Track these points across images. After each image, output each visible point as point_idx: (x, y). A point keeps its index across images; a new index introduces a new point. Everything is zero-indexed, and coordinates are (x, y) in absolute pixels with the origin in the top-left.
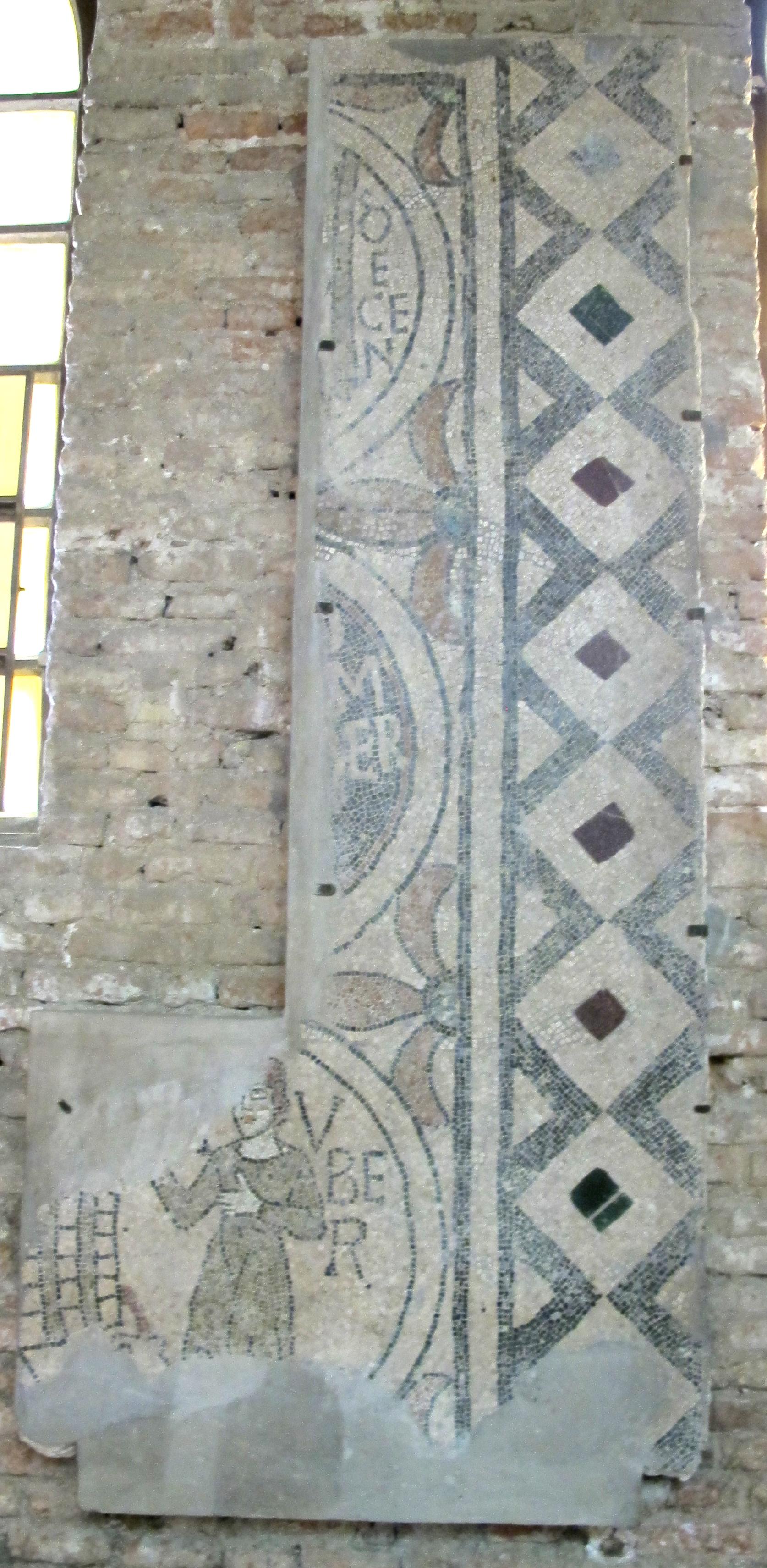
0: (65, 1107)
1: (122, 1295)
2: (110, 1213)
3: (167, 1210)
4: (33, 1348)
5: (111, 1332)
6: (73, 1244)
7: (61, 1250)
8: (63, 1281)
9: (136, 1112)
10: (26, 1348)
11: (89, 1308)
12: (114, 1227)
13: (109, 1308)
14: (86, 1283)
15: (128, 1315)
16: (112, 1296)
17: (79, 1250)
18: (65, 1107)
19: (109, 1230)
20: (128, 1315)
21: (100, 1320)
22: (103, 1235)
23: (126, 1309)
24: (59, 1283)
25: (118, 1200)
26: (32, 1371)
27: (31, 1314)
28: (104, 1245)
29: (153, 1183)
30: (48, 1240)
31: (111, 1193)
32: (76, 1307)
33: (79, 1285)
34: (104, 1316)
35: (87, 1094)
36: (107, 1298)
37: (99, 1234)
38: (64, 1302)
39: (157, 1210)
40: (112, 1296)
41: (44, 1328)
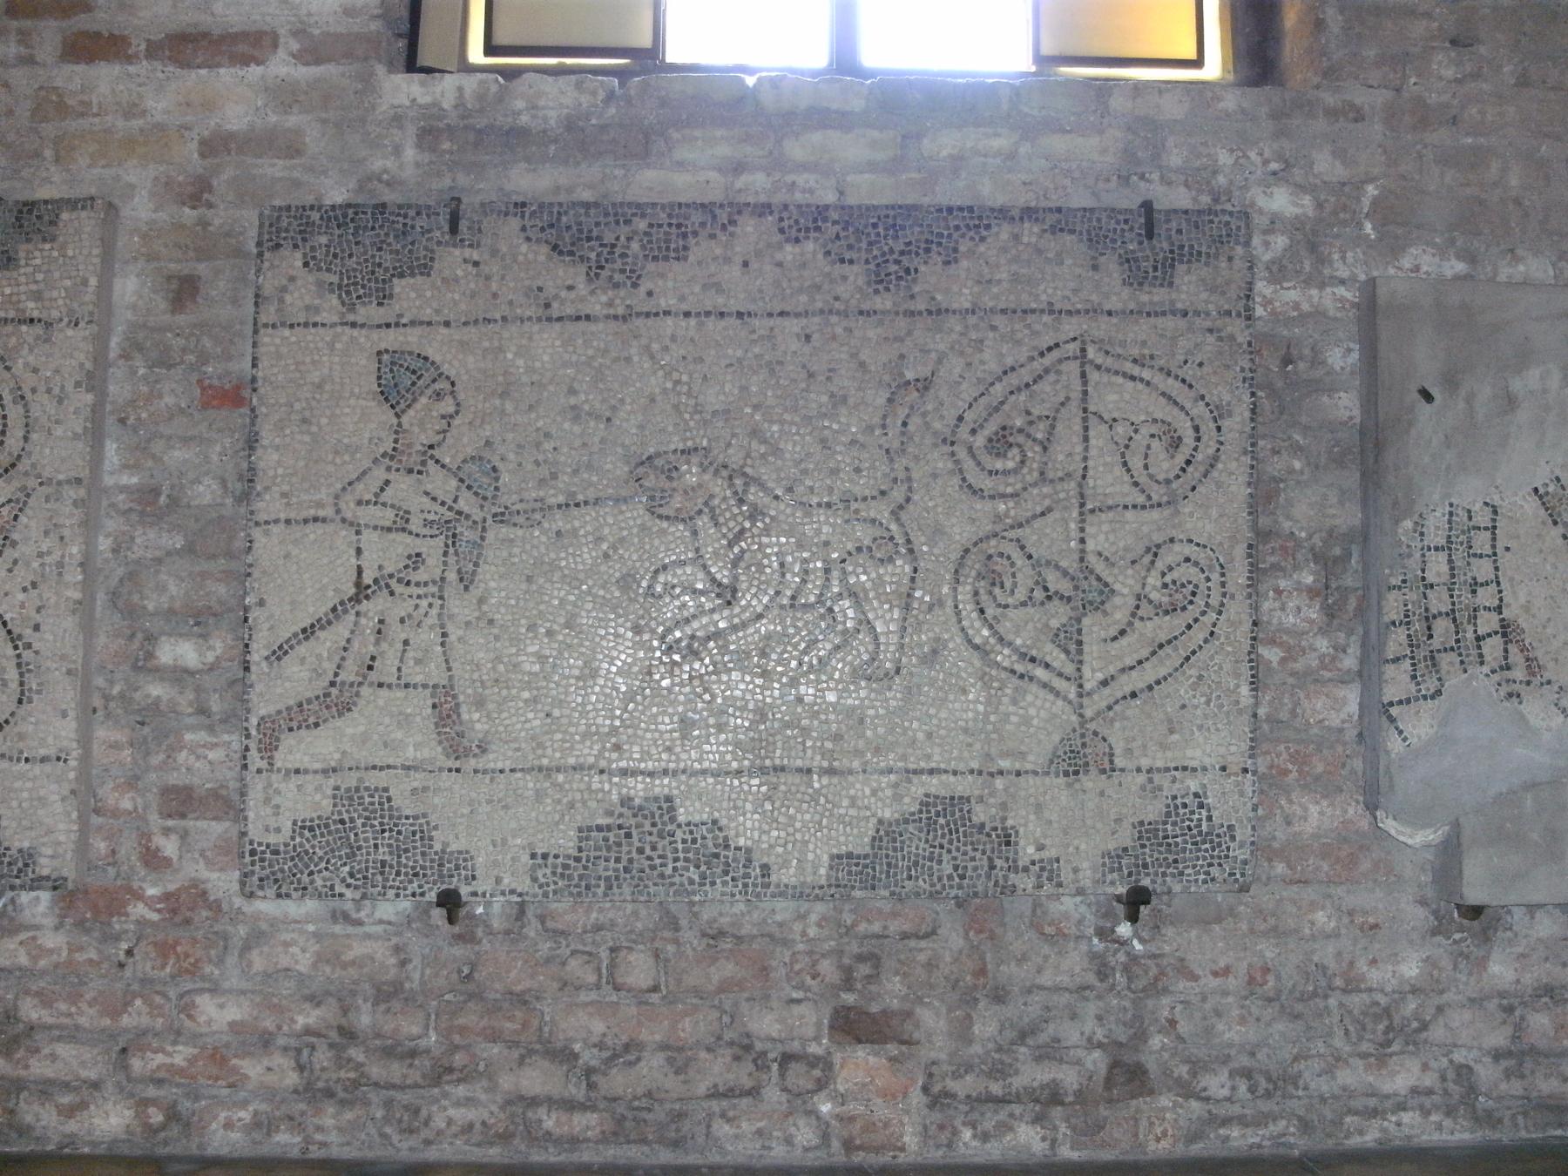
0: (1427, 396)
1: (1506, 630)
2: (1486, 529)
3: (1555, 523)
4: (1400, 702)
5: (1496, 677)
6: (1445, 568)
7: (1431, 577)
8: (1434, 617)
9: (1510, 402)
10: (1391, 704)
11: (1468, 652)
12: (1494, 547)
13: (1493, 647)
14: (1462, 617)
15: (1516, 656)
16: (1496, 633)
17: (1453, 576)
18: (1427, 396)
19: (1488, 550)
20: (1516, 656)
21: (1482, 663)
22: (1481, 556)
23: (1513, 649)
24: (1429, 619)
25: (1495, 512)
26: (1401, 732)
27: (1397, 660)
28: (1483, 570)
29: (1536, 490)
30: (1414, 563)
31: (1486, 504)
32: (1452, 649)
33: (1455, 620)
34: (1487, 658)
35: (1451, 381)
36: (1489, 635)
37: (1475, 555)
38: (1436, 643)
39: (1544, 523)
40: (1496, 633)
41: (1414, 677)
